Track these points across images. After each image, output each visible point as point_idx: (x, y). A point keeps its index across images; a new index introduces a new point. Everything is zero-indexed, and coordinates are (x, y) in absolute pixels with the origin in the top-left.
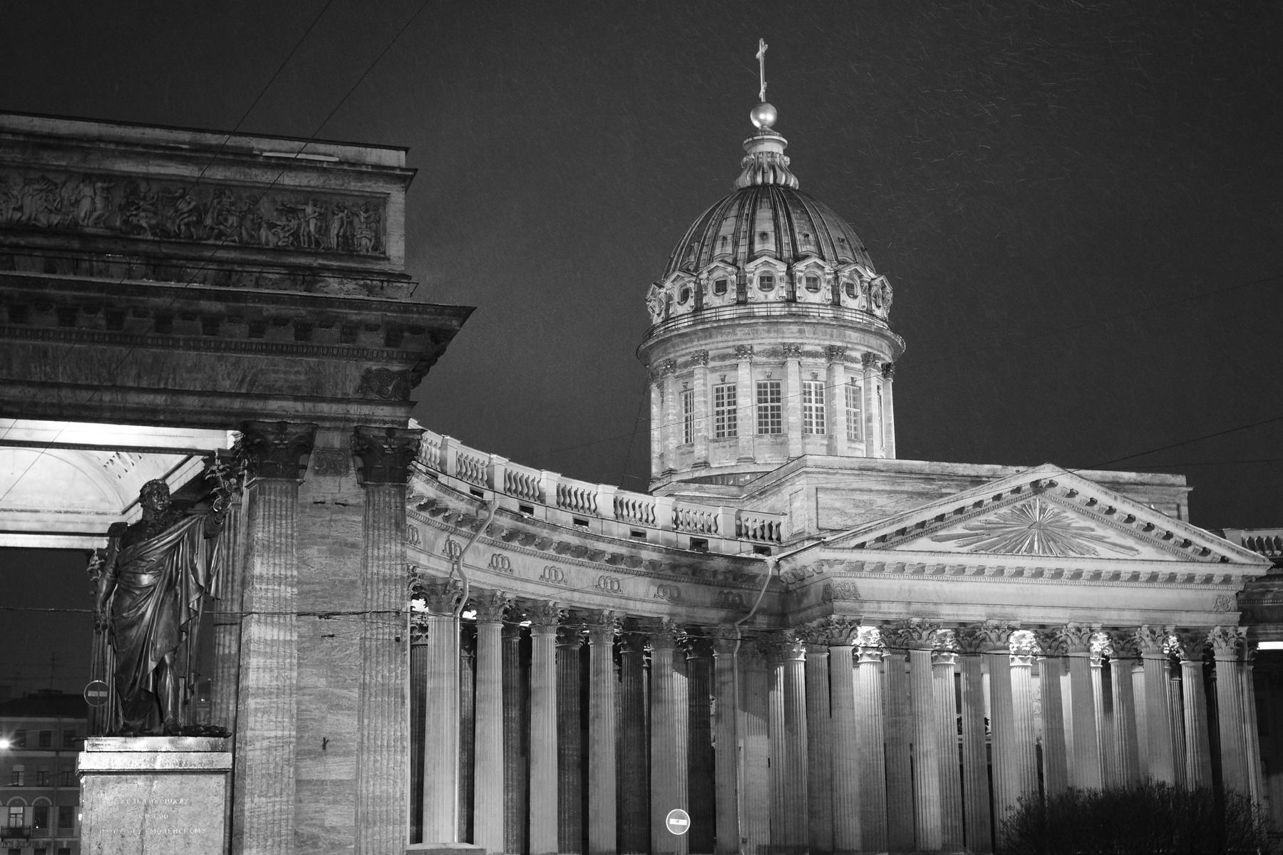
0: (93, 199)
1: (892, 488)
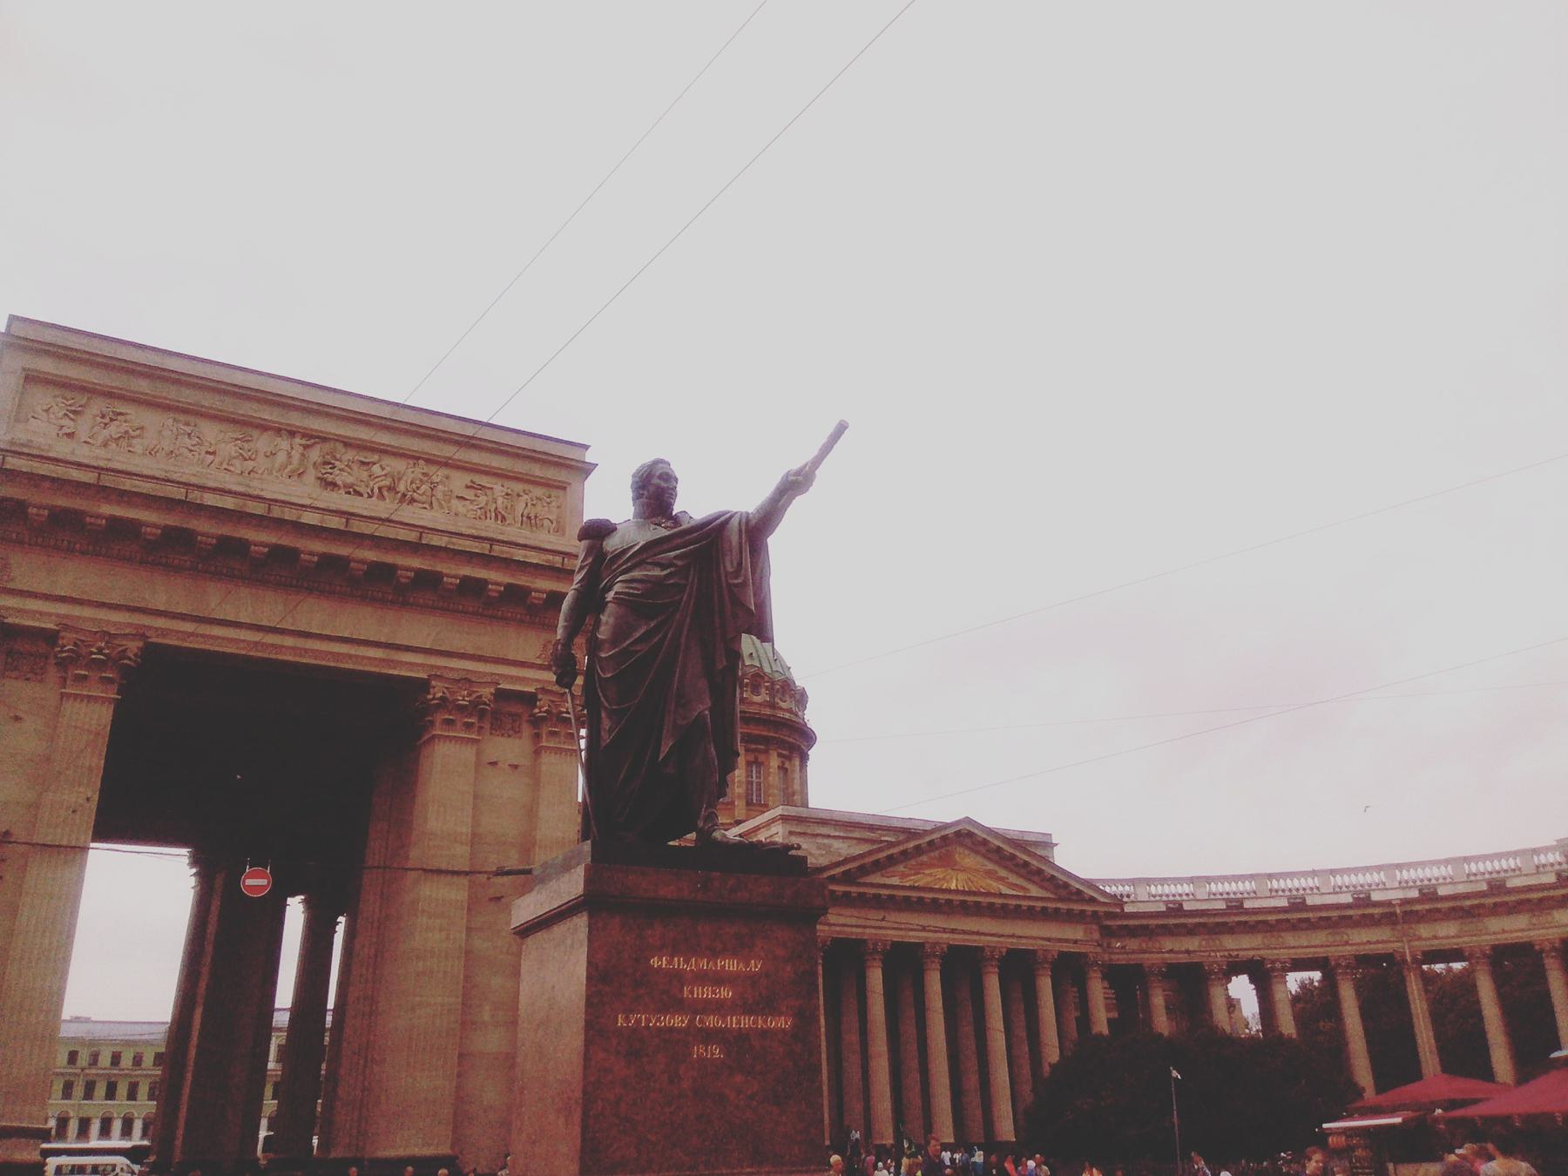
0: (289, 453)
1: (845, 835)
